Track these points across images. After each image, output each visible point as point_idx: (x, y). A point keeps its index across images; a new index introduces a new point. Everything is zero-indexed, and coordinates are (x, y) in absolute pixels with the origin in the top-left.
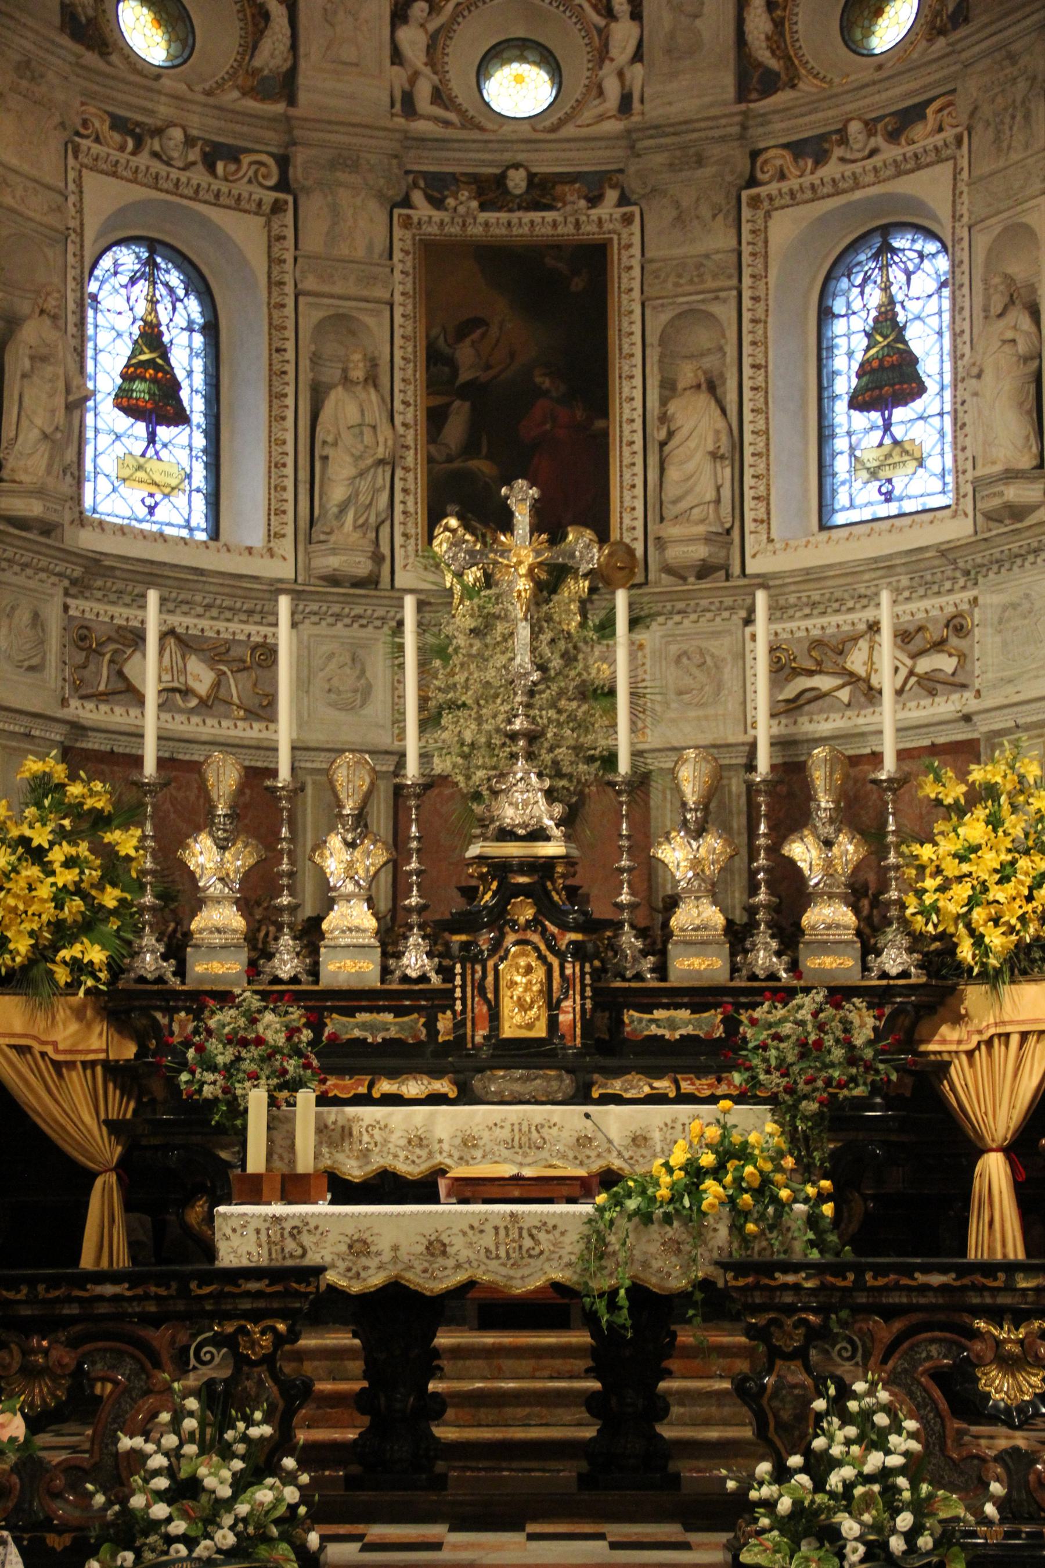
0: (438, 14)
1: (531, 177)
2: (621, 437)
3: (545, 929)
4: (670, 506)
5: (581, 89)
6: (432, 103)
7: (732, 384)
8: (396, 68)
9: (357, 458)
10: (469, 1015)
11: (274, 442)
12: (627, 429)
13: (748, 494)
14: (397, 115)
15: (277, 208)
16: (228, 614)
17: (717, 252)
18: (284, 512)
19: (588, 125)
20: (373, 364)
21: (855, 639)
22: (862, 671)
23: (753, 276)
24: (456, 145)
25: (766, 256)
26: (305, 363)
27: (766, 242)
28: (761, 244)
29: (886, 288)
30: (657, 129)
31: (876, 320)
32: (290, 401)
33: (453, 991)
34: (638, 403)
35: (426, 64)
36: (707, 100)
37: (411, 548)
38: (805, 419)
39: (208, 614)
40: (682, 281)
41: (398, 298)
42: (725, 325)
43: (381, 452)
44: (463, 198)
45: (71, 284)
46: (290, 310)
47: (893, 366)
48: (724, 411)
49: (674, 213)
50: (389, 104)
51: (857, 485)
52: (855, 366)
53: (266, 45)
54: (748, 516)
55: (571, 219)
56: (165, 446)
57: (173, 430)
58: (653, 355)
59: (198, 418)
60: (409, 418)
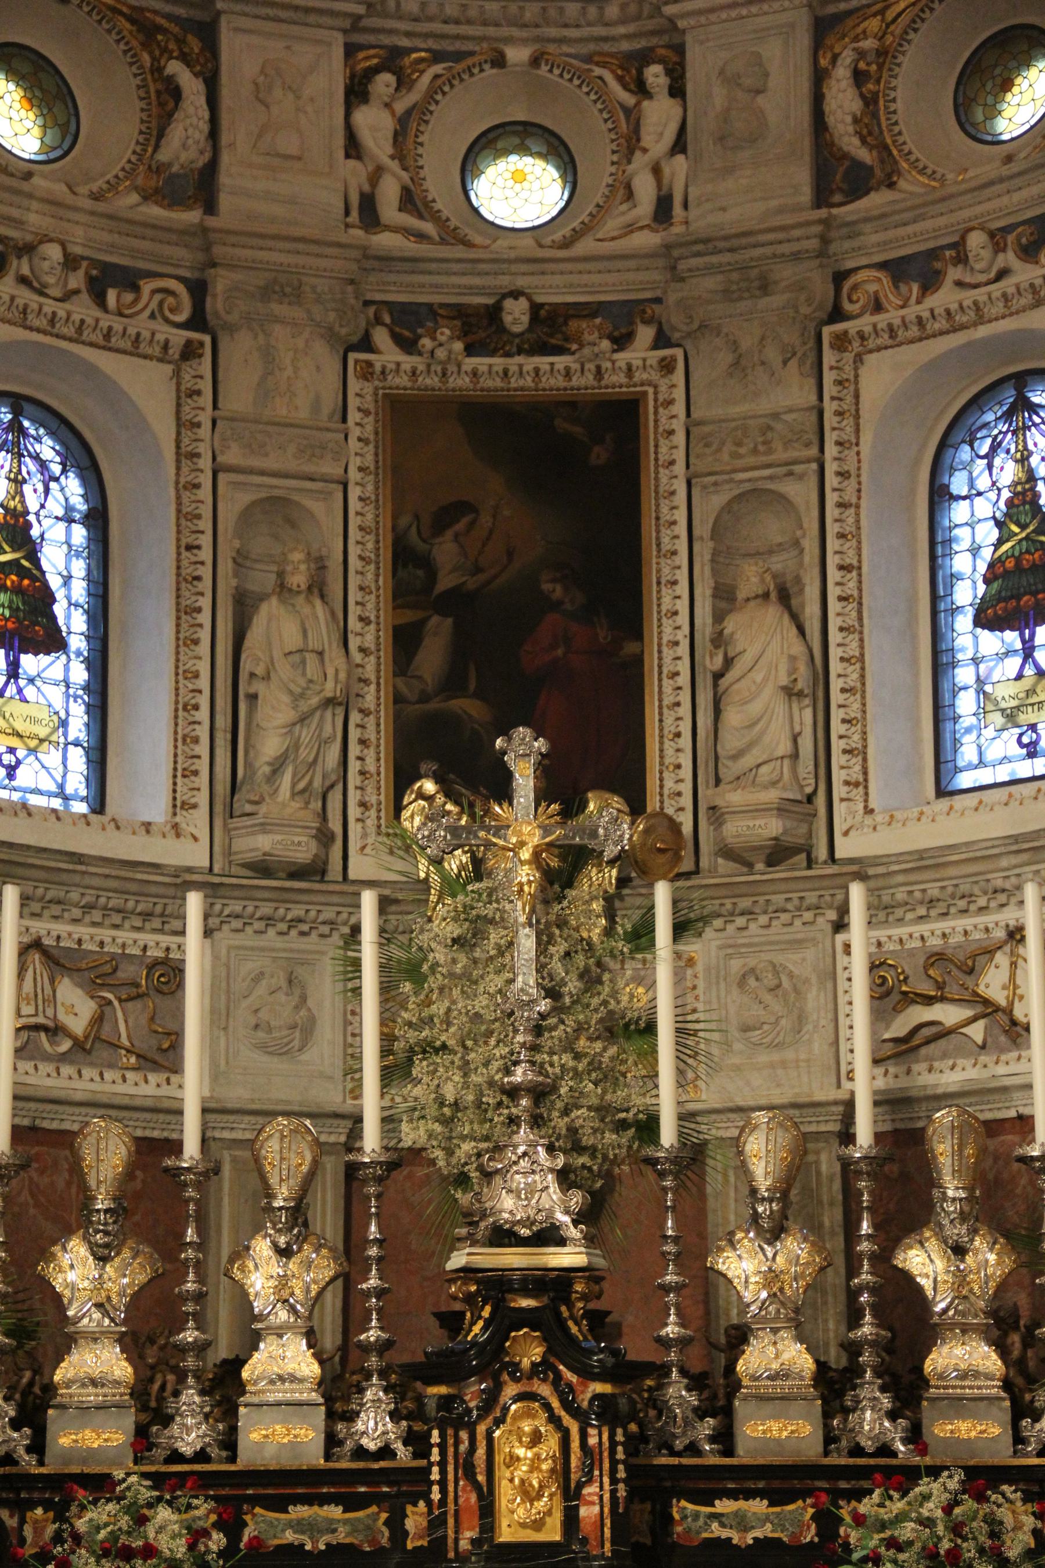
0: (409, 90)
1: (535, 308)
2: (660, 667)
3: (558, 1376)
4: (729, 763)
5: (603, 190)
6: (400, 210)
7: (812, 592)
8: (352, 163)
9: (297, 698)
10: (451, 1507)
11: (183, 674)
12: (668, 653)
13: (836, 746)
14: (353, 226)
15: (190, 352)
16: (117, 919)
17: (791, 411)
18: (196, 773)
19: (613, 239)
20: (320, 565)
21: (990, 952)
22: (1000, 997)
23: (839, 443)
24: (434, 266)
25: (857, 416)
26: (226, 566)
27: (857, 396)
28: (849, 399)
29: (1023, 459)
30: (706, 243)
31: (1009, 503)
32: (205, 618)
33: (427, 1471)
34: (683, 619)
35: (392, 157)
36: (774, 203)
37: (371, 823)
38: (914, 637)
39: (87, 919)
40: (742, 451)
41: (354, 475)
42: (802, 508)
43: (330, 689)
44: (443, 339)
46: (205, 493)
47: (1034, 567)
48: (801, 631)
49: (730, 358)
50: (342, 211)
51: (989, 732)
52: (982, 567)
54: (838, 776)
55: (590, 366)
56: (31, 681)
57: (44, 659)
58: (704, 551)
59: (77, 643)
60: (369, 641)
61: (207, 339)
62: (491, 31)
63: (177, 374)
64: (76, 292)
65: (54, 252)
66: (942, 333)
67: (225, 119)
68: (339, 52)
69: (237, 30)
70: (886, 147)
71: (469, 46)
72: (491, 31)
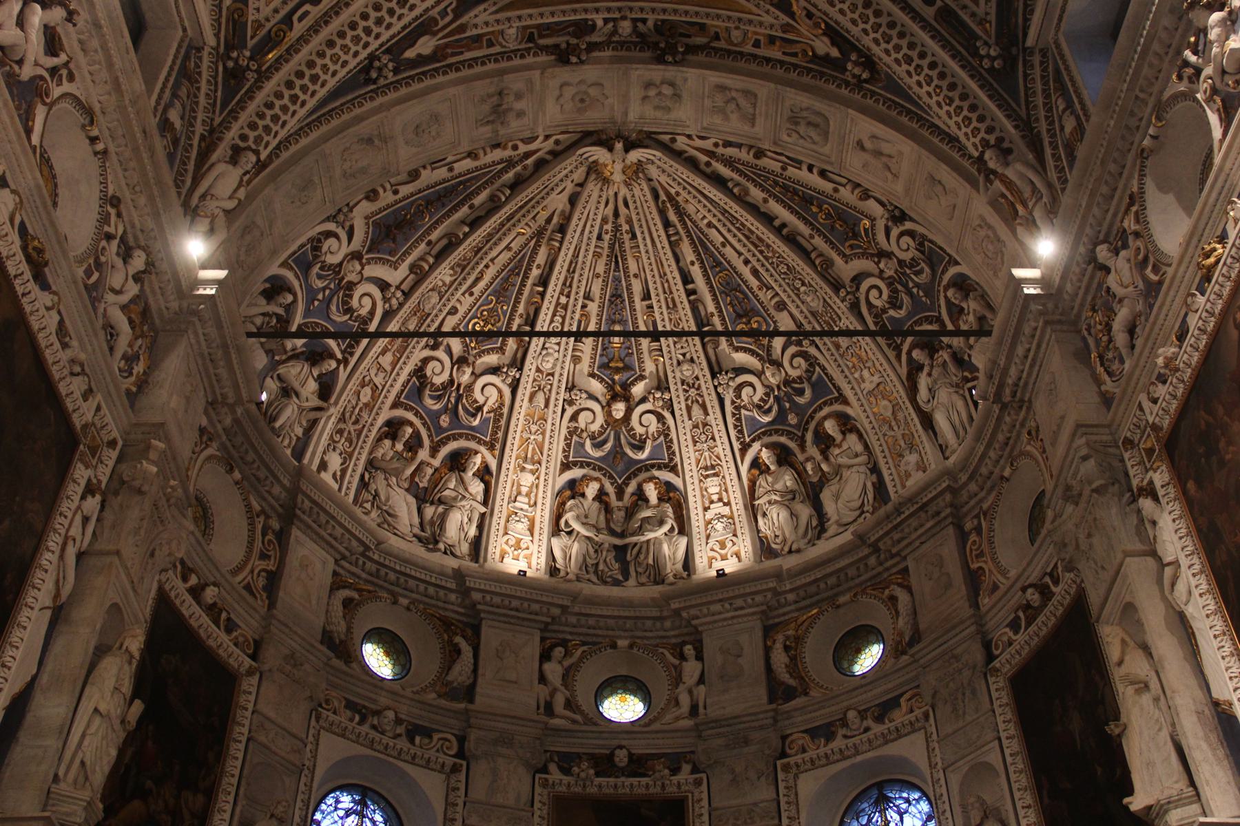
1: (631, 755)
15: (455, 769)
25: (797, 805)
27: (796, 794)
30: (717, 723)
45: (299, 804)
53: (457, 668)
55: (659, 783)
61: (464, 763)
62: (610, 633)
63: (448, 778)
64: (400, 735)
65: (390, 715)
66: (838, 761)
67: (481, 663)
68: (537, 639)
70: (802, 678)
71: (600, 640)
72: (610, 633)
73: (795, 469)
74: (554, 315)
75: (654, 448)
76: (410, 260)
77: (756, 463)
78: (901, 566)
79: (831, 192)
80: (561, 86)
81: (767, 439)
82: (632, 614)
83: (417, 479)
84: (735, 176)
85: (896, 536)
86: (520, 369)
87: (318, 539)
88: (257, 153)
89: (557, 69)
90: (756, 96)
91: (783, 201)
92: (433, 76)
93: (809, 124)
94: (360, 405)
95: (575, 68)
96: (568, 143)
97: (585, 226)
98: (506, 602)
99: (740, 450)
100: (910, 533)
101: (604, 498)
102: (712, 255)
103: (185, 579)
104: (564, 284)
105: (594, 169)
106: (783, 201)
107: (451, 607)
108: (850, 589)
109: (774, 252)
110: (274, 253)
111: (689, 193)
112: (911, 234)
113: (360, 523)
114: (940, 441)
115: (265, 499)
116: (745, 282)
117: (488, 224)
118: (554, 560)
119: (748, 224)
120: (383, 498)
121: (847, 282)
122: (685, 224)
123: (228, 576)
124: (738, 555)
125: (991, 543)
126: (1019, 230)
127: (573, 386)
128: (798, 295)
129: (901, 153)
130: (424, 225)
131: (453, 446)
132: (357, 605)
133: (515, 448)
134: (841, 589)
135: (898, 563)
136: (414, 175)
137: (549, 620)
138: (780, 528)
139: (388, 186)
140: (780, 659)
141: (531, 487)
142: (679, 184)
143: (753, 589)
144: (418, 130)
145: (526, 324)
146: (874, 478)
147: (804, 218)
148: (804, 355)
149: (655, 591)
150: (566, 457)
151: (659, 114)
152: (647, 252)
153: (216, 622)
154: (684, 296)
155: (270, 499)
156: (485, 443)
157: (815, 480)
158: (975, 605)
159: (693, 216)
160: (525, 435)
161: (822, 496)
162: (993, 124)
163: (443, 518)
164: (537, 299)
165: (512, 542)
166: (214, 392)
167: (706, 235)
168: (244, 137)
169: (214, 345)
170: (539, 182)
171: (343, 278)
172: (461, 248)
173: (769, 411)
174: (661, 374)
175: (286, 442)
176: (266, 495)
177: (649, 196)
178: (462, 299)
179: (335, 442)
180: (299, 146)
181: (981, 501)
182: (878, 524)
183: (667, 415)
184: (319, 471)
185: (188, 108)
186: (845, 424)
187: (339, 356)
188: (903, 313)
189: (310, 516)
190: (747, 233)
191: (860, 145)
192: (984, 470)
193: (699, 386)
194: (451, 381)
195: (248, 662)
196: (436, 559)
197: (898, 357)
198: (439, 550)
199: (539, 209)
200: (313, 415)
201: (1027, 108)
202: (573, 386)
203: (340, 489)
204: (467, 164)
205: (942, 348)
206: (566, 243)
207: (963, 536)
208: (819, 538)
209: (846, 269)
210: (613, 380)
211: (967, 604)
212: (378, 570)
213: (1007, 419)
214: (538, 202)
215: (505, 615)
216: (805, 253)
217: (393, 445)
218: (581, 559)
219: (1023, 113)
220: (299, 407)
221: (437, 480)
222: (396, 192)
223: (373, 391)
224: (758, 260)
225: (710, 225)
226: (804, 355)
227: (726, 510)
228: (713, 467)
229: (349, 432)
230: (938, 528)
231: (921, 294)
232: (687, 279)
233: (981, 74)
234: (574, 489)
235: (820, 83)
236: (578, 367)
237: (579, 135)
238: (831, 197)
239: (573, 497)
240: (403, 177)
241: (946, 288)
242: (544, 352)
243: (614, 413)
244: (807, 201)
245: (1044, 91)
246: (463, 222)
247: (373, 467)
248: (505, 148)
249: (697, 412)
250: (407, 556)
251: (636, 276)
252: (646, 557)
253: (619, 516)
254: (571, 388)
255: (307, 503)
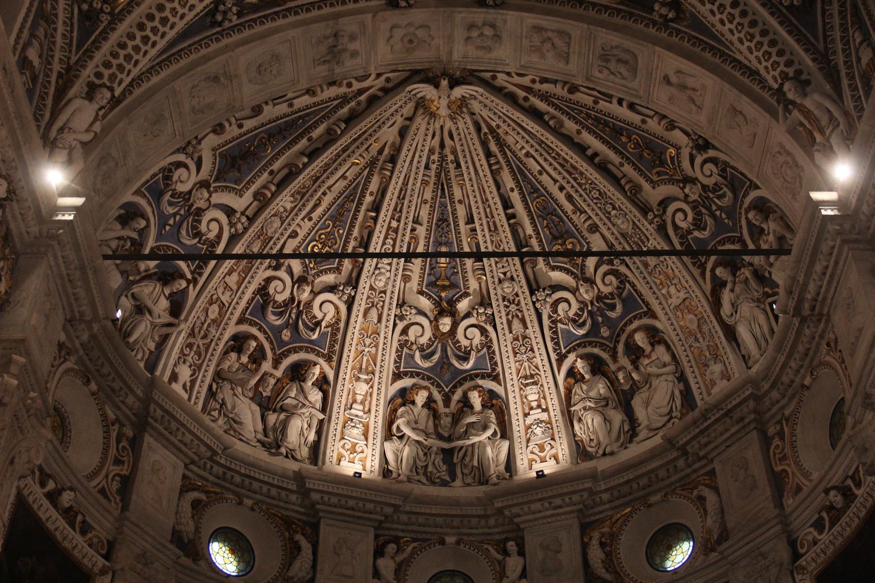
8: (376, 580)
53: (297, 565)
62: (439, 530)
67: (320, 559)
68: (372, 536)
69: (327, 525)
70: (618, 573)
72: (439, 530)
73: (608, 378)
74: (386, 238)
75: (477, 359)
76: (253, 188)
77: (571, 373)
78: (708, 468)
79: (639, 124)
80: (392, 28)
81: (581, 351)
82: (459, 512)
83: (260, 389)
84: (551, 110)
85: (704, 440)
86: (355, 288)
87: (169, 445)
88: (111, 90)
89: (388, 13)
90: (570, 36)
91: (595, 133)
92: (274, 19)
93: (619, 61)
94: (209, 321)
95: (403, 11)
96: (397, 81)
97: (413, 157)
98: (343, 502)
99: (557, 360)
100: (716, 438)
101: (432, 405)
102: (530, 183)
103: (43, 484)
104: (395, 209)
105: (421, 104)
106: (595, 133)
107: (292, 507)
108: (660, 490)
109: (587, 179)
110: (128, 182)
111: (509, 125)
112: (714, 161)
113: (208, 430)
114: (743, 353)
115: (119, 409)
116: (560, 207)
117: (325, 155)
118: (387, 462)
119: (563, 154)
120: (229, 407)
121: (655, 206)
122: (505, 154)
123: (84, 481)
124: (556, 457)
125: (793, 447)
126: (817, 156)
127: (404, 303)
128: (609, 219)
129: (704, 87)
130: (266, 156)
131: (293, 358)
132: (205, 505)
133: (351, 360)
134: (652, 489)
135: (705, 465)
136: (257, 110)
137: (382, 518)
138: (595, 432)
139: (233, 120)
140: (596, 554)
141: (365, 396)
142: (500, 117)
143: (571, 489)
144: (260, 69)
145: (360, 246)
146: (681, 386)
147: (615, 148)
148: (615, 273)
149: (480, 491)
150: (398, 368)
151: (481, 53)
152: (470, 180)
153: (72, 525)
154: (504, 220)
155: (124, 408)
156: (323, 356)
157: (626, 387)
158: (780, 506)
159: (513, 147)
160: (360, 348)
161: (632, 402)
162: (792, 57)
163: (285, 424)
164: (370, 223)
165: (348, 446)
166: (72, 311)
167: (524, 164)
168: (99, 75)
169: (72, 266)
170: (372, 116)
171: (192, 205)
172: (301, 177)
173: (583, 324)
174: (484, 291)
175: (139, 356)
176: (121, 405)
177: (472, 129)
178: (302, 223)
179: (186, 355)
180: (151, 83)
181: (783, 407)
182: (686, 429)
183: (489, 328)
184: (170, 382)
185: (46, 47)
186: (653, 337)
187: (189, 276)
188: (706, 234)
189: (161, 424)
190: (561, 161)
191: (667, 80)
192: (785, 379)
193: (519, 301)
194: (292, 299)
195: (101, 561)
196: (279, 462)
197: (703, 274)
198: (281, 454)
199: (372, 141)
200: (165, 330)
201: (825, 42)
202: (404, 303)
203: (189, 399)
204: (306, 100)
205: (744, 266)
206: (396, 172)
207: (766, 441)
208: (631, 442)
209: (653, 194)
210: (440, 297)
211: (772, 505)
212: (224, 473)
213: (807, 332)
214: (371, 135)
215: (341, 514)
216: (615, 180)
217: (239, 358)
218: (411, 462)
219: (821, 46)
220: (152, 323)
221: (279, 389)
222: (240, 126)
223: (221, 308)
224: (573, 187)
225: (528, 155)
226: (615, 273)
227: (544, 416)
228: (532, 376)
229: (198, 346)
230: (743, 433)
231: (724, 216)
232: (507, 204)
233: (780, 11)
234: (404, 397)
235: (630, 23)
236: (408, 285)
237: (408, 74)
238: (639, 128)
239: (404, 405)
240: (247, 112)
241: (747, 211)
242: (377, 272)
243: (441, 327)
244: (617, 132)
245: (841, 25)
246: (302, 153)
247: (220, 378)
248: (340, 85)
249: (517, 325)
250: (252, 459)
251: (460, 202)
252: (472, 460)
253: (446, 421)
254: (401, 304)
255: (159, 412)
